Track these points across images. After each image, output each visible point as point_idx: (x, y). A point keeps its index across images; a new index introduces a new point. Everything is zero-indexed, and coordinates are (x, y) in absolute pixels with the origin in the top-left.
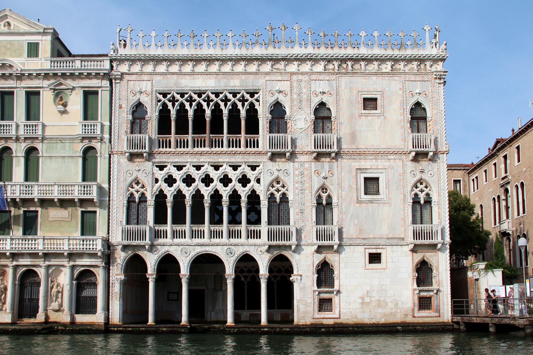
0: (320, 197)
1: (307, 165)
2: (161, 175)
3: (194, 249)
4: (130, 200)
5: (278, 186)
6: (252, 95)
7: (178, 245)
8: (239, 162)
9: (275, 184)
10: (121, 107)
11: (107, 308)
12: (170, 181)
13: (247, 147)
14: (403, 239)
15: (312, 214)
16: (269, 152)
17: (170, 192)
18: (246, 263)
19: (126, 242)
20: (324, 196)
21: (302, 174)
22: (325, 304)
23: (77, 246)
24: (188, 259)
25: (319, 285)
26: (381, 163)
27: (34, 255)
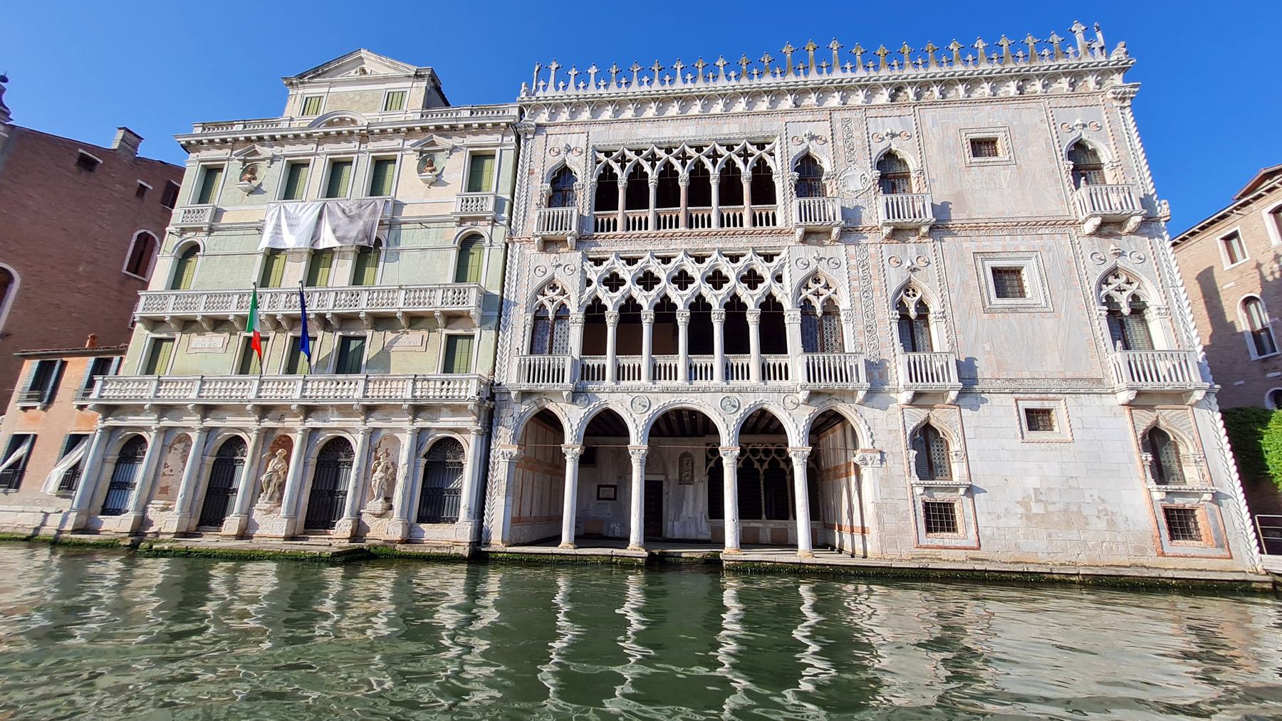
0: (901, 306)
2: (595, 273)
4: (539, 317)
5: (818, 286)
6: (761, 146)
9: (811, 284)
10: (531, 173)
11: (479, 512)
12: (613, 282)
14: (1100, 381)
17: (612, 301)
19: (525, 386)
22: (939, 517)
23: (432, 392)
26: (1022, 242)
27: (345, 410)
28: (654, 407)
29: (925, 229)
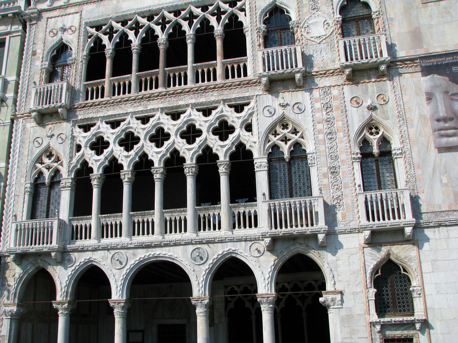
0: (365, 143)
1: (335, 92)
2: (83, 138)
3: (134, 255)
5: (285, 131)
7: (106, 249)
8: (214, 102)
9: (279, 129)
12: (99, 145)
13: (227, 77)
15: (353, 173)
16: (264, 76)
17: (97, 162)
18: (232, 273)
19: (20, 249)
20: (374, 140)
21: (328, 107)
24: (124, 271)
25: (381, 309)
28: (132, 262)
29: (383, 67)
